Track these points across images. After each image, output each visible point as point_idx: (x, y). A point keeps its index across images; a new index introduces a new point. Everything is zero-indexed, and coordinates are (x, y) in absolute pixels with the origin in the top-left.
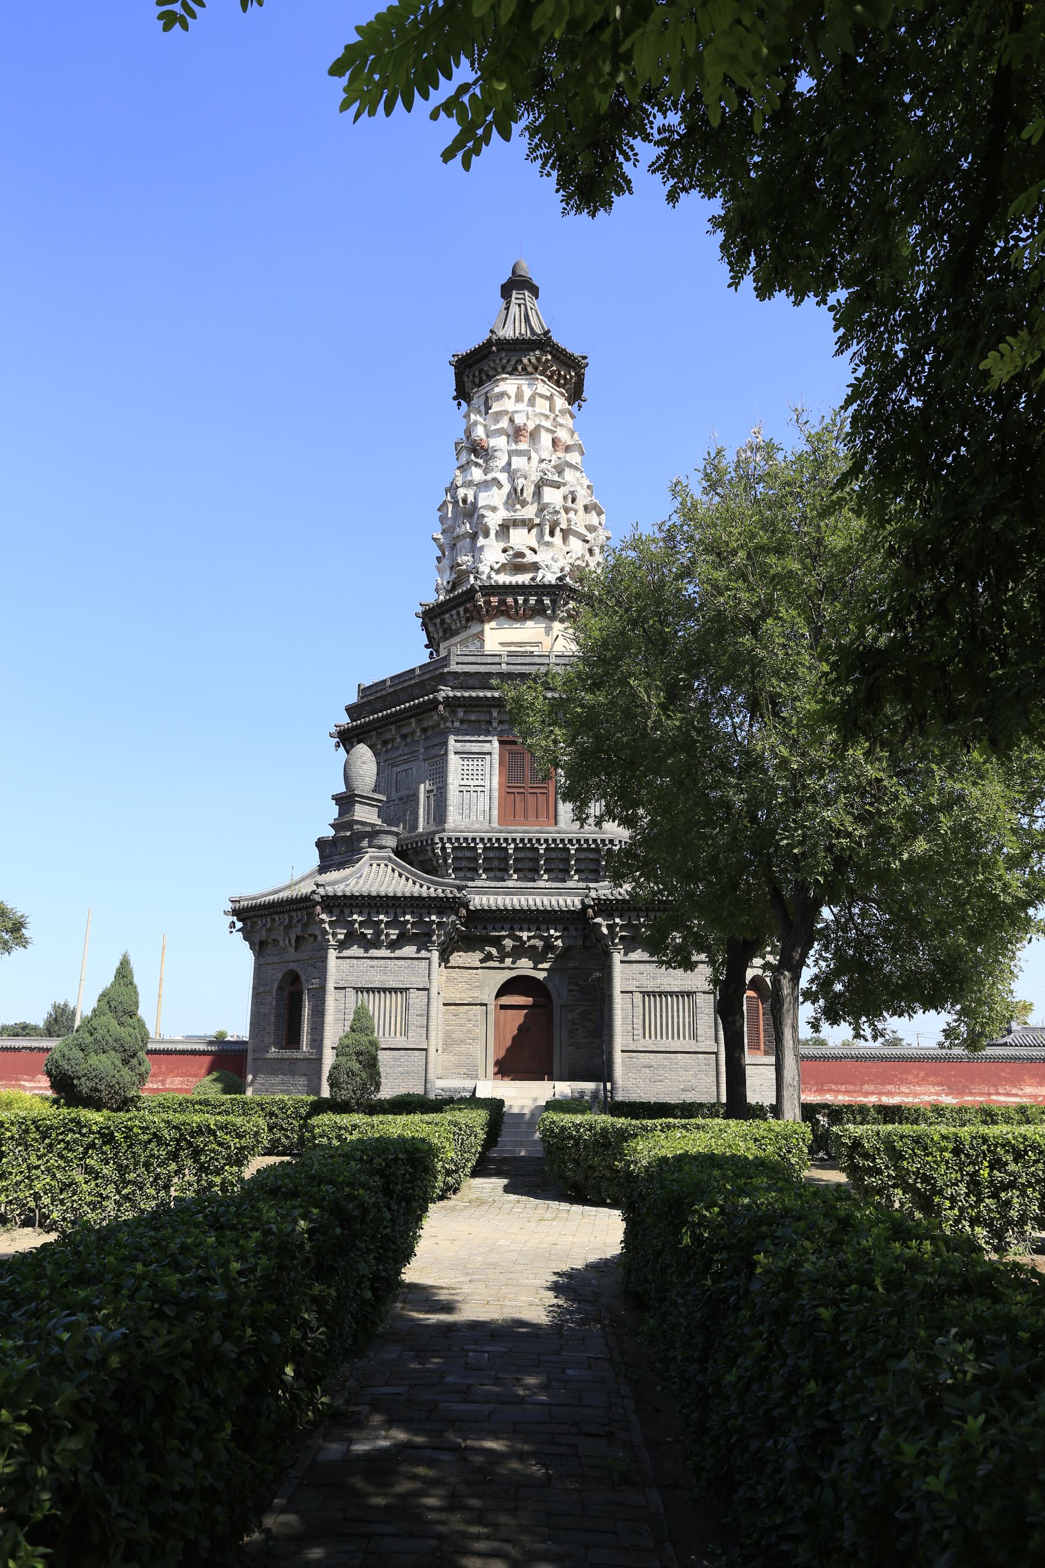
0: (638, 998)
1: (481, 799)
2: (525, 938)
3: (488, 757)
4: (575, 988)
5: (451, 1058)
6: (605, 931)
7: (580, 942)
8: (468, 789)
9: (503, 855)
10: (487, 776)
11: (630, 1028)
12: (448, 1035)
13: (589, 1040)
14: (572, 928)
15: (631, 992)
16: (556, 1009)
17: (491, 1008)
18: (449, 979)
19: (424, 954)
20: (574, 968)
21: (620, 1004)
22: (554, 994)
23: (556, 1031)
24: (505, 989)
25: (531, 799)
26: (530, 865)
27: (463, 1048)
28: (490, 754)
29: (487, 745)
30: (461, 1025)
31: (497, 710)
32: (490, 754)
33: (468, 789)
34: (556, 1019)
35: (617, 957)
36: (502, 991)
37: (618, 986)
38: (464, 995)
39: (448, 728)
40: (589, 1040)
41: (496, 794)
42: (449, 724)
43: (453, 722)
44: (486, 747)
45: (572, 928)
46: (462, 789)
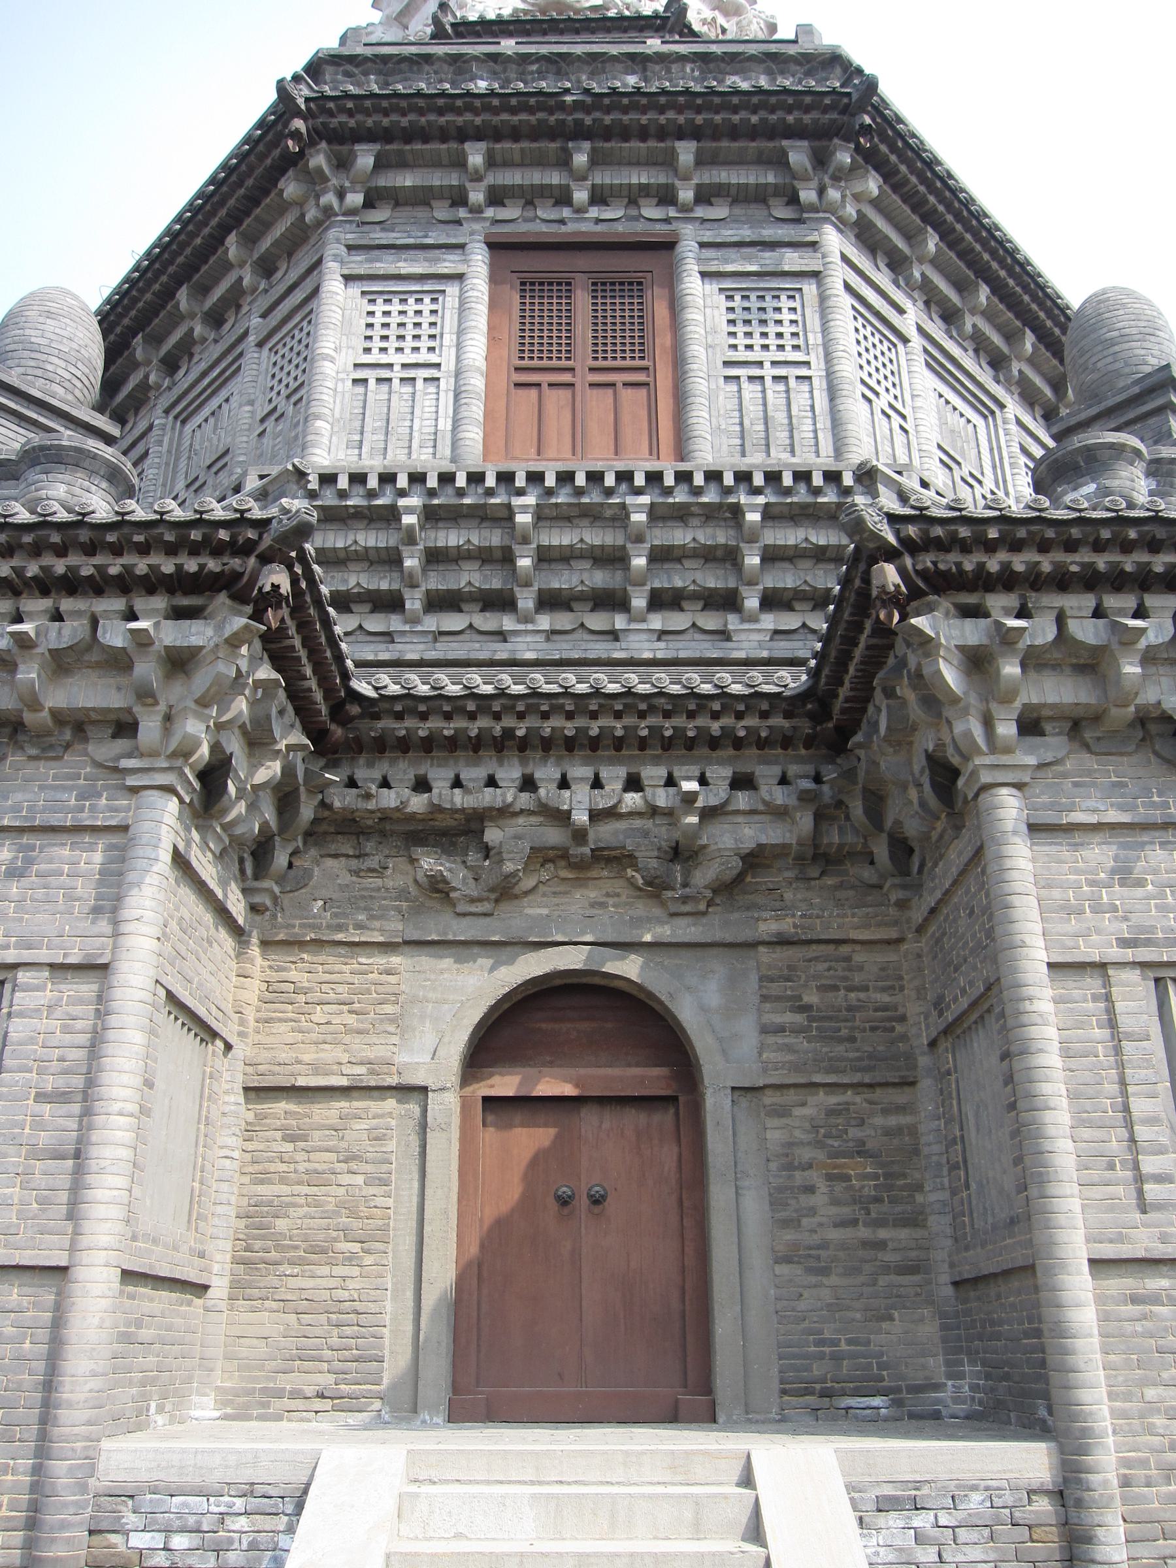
0: (1134, 998)
1: (425, 403)
2: (581, 817)
3: (452, 290)
4: (789, 1018)
5: (269, 1321)
6: (951, 675)
7: (805, 821)
8: (385, 374)
9: (494, 538)
10: (449, 339)
11: (1115, 1144)
12: (257, 1218)
13: (864, 1232)
14: (767, 774)
15: (1101, 967)
16: (716, 1103)
17: (446, 1105)
18: (273, 993)
19: (104, 809)
20: (783, 941)
21: (1048, 1016)
22: (703, 1043)
23: (719, 1195)
24: (500, 1036)
25: (598, 404)
26: (599, 579)
27: (319, 1281)
28: (460, 277)
29: (454, 256)
30: (316, 1178)
31: (482, 146)
32: (460, 277)
33: (385, 374)
34: (717, 1144)
35: (1009, 808)
36: (491, 1043)
37: (1034, 942)
38: (330, 1054)
39: (328, 211)
40: (864, 1232)
41: (477, 383)
42: (329, 198)
43: (341, 195)
44: (448, 264)
45: (767, 774)
46: (360, 374)
